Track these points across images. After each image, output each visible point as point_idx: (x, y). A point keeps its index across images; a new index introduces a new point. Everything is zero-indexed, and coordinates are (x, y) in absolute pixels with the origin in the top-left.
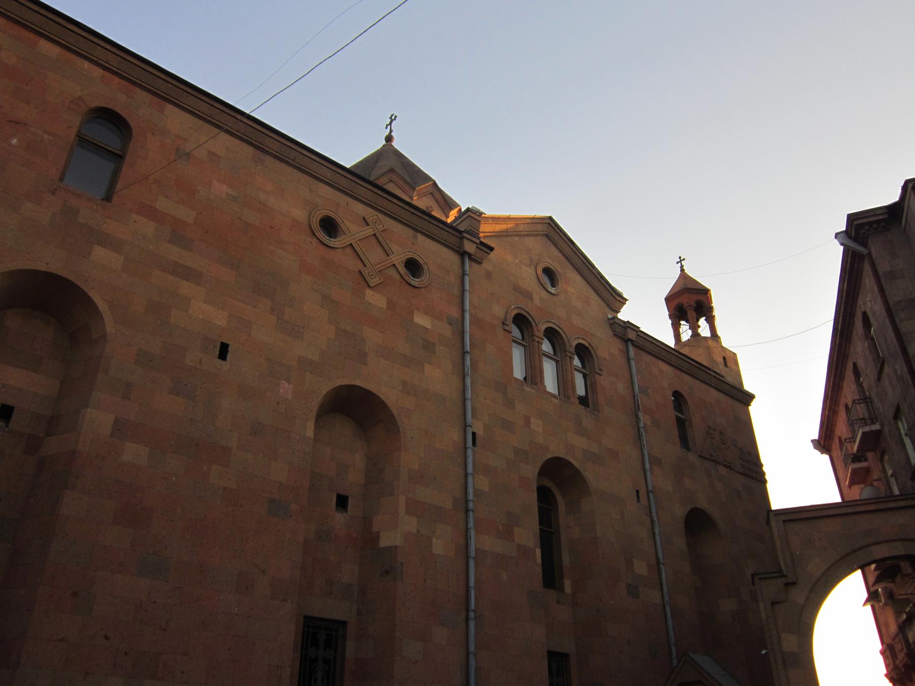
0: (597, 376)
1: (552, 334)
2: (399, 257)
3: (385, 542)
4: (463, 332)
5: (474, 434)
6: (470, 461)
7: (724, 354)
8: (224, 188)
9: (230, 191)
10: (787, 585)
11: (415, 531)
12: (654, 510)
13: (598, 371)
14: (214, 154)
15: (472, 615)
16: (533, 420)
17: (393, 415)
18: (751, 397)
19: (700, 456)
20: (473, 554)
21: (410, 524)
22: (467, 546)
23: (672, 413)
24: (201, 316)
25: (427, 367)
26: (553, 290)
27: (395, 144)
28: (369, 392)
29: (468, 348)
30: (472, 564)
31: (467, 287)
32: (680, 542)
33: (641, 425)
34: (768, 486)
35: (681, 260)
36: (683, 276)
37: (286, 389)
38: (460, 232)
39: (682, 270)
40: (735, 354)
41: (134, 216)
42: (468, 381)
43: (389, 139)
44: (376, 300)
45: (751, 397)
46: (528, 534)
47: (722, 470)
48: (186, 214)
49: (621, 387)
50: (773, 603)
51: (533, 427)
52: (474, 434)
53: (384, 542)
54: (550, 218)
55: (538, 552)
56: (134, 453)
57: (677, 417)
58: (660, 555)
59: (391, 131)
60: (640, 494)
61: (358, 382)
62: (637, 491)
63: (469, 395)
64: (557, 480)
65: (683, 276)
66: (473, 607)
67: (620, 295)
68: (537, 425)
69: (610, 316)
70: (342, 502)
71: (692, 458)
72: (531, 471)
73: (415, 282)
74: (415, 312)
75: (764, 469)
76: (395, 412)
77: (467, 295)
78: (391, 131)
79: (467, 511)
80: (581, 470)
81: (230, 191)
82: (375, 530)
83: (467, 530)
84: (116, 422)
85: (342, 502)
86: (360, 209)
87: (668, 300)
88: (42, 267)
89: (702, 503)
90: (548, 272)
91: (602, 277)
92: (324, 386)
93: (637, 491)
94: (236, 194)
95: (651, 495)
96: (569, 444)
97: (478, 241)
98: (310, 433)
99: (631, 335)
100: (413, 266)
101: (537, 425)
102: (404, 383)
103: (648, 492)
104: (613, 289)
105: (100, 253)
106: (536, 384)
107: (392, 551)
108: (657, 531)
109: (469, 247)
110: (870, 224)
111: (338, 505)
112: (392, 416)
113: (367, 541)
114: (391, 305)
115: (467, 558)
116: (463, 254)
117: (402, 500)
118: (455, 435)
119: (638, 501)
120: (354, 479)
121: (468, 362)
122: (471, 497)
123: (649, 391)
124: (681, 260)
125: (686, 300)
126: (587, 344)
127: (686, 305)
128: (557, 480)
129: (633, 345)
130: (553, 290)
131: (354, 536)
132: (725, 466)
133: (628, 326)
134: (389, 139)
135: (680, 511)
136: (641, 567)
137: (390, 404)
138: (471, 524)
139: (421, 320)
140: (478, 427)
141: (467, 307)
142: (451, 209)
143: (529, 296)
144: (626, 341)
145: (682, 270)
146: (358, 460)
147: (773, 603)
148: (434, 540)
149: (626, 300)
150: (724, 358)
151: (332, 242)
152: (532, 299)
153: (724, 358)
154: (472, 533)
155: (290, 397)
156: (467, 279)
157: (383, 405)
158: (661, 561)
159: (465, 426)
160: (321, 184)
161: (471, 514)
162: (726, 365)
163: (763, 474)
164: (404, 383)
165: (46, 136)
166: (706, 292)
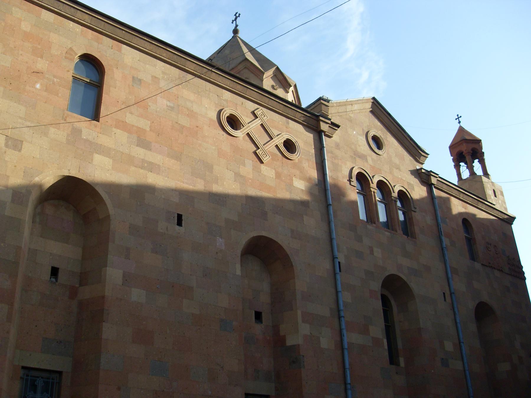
0: (413, 213)
1: (381, 185)
2: (279, 141)
3: (290, 342)
6: (339, 283)
7: (493, 188)
8: (165, 102)
9: (169, 104)
11: (309, 334)
12: (455, 306)
13: (413, 209)
14: (156, 77)
15: (349, 386)
16: (375, 249)
17: (287, 255)
18: (513, 218)
19: (482, 264)
20: (346, 346)
21: (305, 329)
22: (342, 340)
23: (462, 234)
24: (163, 197)
25: (305, 218)
27: (240, 35)
28: (271, 240)
30: (346, 352)
32: (473, 327)
34: (527, 281)
35: (458, 118)
36: (461, 130)
37: (220, 242)
41: (114, 129)
43: (236, 31)
45: (513, 218)
46: (377, 330)
47: (497, 273)
48: (144, 124)
49: (429, 219)
51: (375, 254)
53: (290, 342)
55: (385, 341)
56: (137, 295)
59: (237, 26)
60: (446, 294)
61: (264, 234)
62: (444, 293)
64: (394, 290)
65: (461, 130)
66: (349, 381)
68: (378, 252)
69: (418, 168)
70: (258, 316)
71: (477, 265)
72: (376, 286)
74: (294, 178)
75: (524, 270)
76: (289, 253)
78: (237, 26)
79: (340, 317)
80: (408, 283)
81: (169, 104)
82: (282, 333)
83: (341, 330)
84: (124, 276)
87: (452, 148)
89: (485, 298)
90: (376, 139)
91: (411, 139)
92: (243, 239)
94: (172, 105)
95: (453, 295)
96: (398, 264)
97: (329, 122)
101: (378, 252)
102: (292, 231)
103: (451, 294)
105: (98, 158)
106: (375, 223)
107: (295, 348)
108: (458, 321)
112: (287, 255)
113: (278, 341)
114: (278, 175)
115: (342, 349)
117: (299, 313)
118: (327, 265)
119: (445, 300)
120: (264, 300)
121: (331, 212)
122: (342, 307)
123: (447, 220)
124: (458, 118)
125: (464, 148)
127: (464, 151)
128: (394, 290)
129: (435, 187)
131: (268, 338)
132: (499, 270)
134: (236, 31)
135: (472, 305)
136: (449, 346)
137: (285, 247)
138: (343, 326)
142: (290, 86)
143: (363, 157)
146: (265, 287)
148: (321, 338)
149: (428, 154)
150: (494, 191)
152: (367, 161)
153: (494, 191)
154: (345, 332)
155: (223, 248)
157: (280, 247)
158: (462, 340)
159: (334, 258)
160: (224, 91)
161: (342, 319)
163: (523, 273)
164: (292, 231)
165: (55, 80)
166: (478, 142)
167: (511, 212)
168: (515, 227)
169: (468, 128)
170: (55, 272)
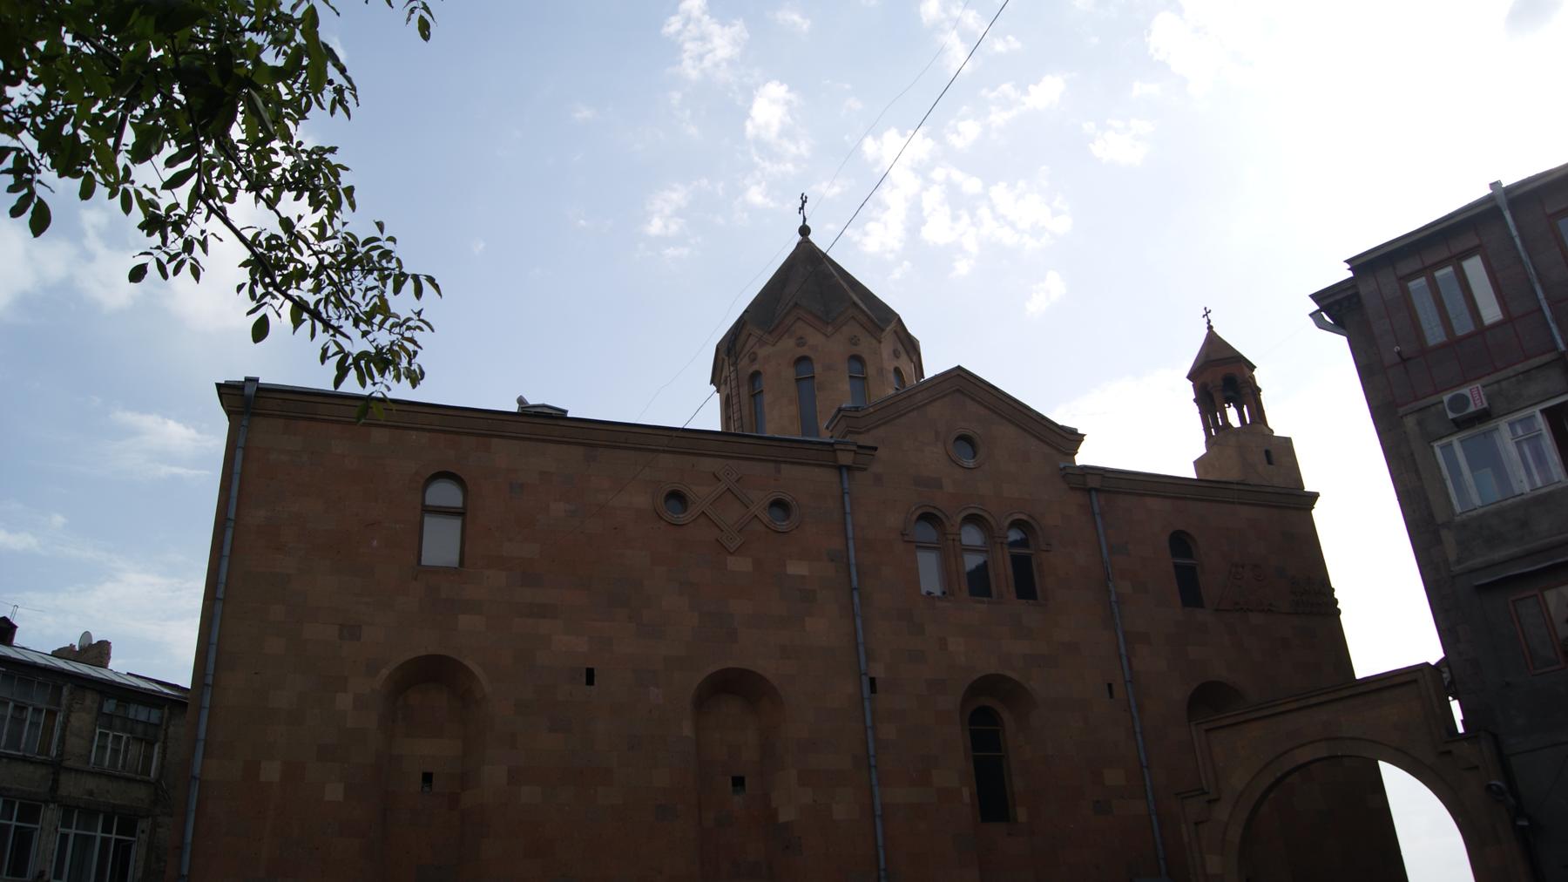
3: (783, 818)
4: (848, 565)
5: (873, 681)
10: (1209, 802)
20: (878, 813)
26: (971, 463)
27: (810, 237)
29: (855, 584)
30: (878, 821)
31: (848, 509)
33: (1113, 598)
34: (1342, 617)
38: (831, 445)
39: (1210, 328)
40: (1288, 441)
42: (859, 622)
43: (805, 231)
44: (740, 565)
46: (954, 774)
50: (1196, 824)
52: (873, 681)
53: (783, 818)
54: (959, 367)
57: (1176, 566)
58: (1142, 755)
61: (731, 664)
62: (1110, 686)
63: (861, 639)
67: (1073, 432)
70: (738, 782)
73: (783, 526)
77: (849, 519)
85: (738, 782)
86: (707, 464)
87: (1190, 377)
88: (423, 652)
93: (1110, 686)
98: (687, 730)
99: (1093, 482)
100: (779, 504)
104: (1062, 428)
109: (845, 458)
110: (1338, 302)
111: (734, 785)
116: (840, 468)
121: (856, 599)
126: (1024, 517)
130: (971, 463)
133: (1087, 470)
134: (805, 231)
138: (874, 781)
139: (796, 568)
140: (878, 671)
141: (850, 535)
144: (1089, 490)
145: (1210, 328)
147: (1196, 824)
150: (1267, 453)
151: (682, 518)
153: (1267, 453)
156: (847, 498)
162: (1270, 462)
163: (1336, 602)
167: (1308, 487)
168: (1318, 513)
169: (1220, 331)
170: (427, 778)
